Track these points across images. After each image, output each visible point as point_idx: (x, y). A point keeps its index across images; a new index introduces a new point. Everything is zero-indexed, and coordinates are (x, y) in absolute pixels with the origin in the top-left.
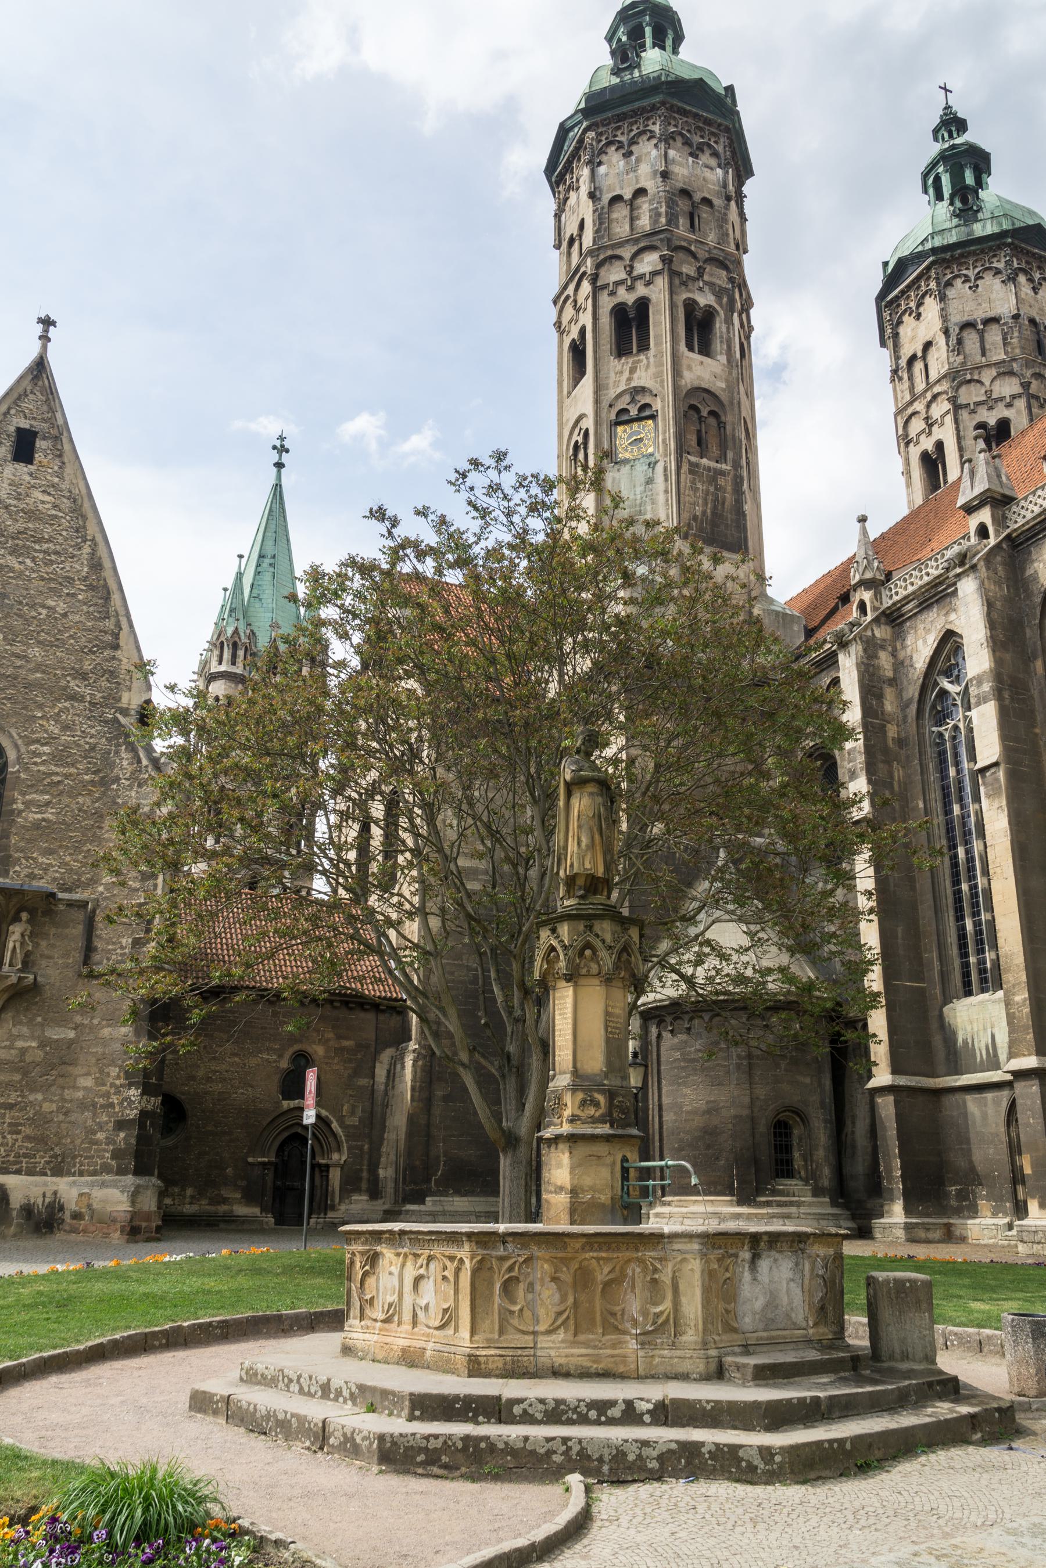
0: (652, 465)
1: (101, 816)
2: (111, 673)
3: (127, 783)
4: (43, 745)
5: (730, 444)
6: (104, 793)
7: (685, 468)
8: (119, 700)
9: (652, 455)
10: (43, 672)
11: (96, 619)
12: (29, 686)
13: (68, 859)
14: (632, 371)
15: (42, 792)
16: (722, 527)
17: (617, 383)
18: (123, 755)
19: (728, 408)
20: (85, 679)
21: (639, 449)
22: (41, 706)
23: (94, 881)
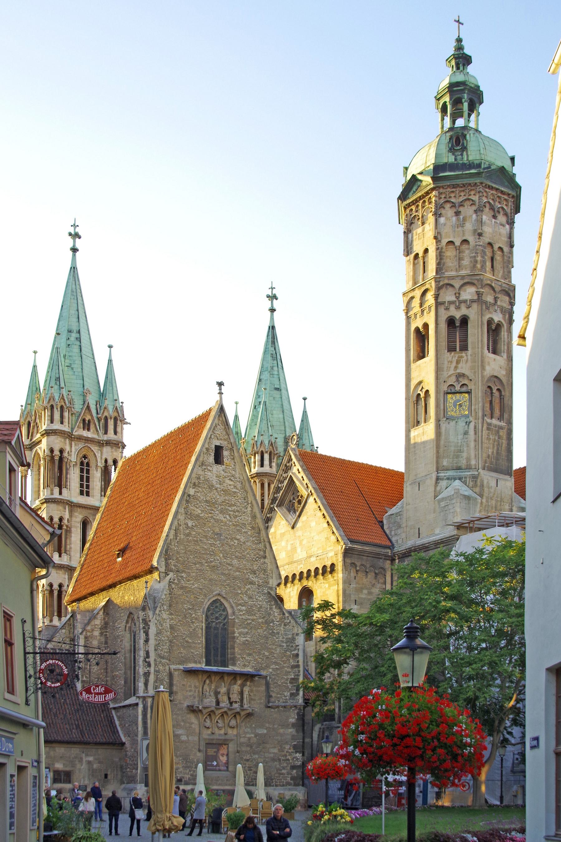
0: (468, 423)
1: (267, 638)
2: (265, 570)
3: (278, 623)
4: (242, 606)
5: (506, 409)
6: (267, 627)
7: (485, 426)
8: (268, 583)
9: (467, 416)
10: (239, 571)
11: (256, 544)
12: (235, 578)
13: (257, 657)
14: (458, 362)
15: (244, 628)
16: (501, 461)
17: (449, 368)
18: (275, 610)
19: (506, 387)
20: (255, 574)
21: (460, 411)
22: (240, 588)
23: (267, 667)
